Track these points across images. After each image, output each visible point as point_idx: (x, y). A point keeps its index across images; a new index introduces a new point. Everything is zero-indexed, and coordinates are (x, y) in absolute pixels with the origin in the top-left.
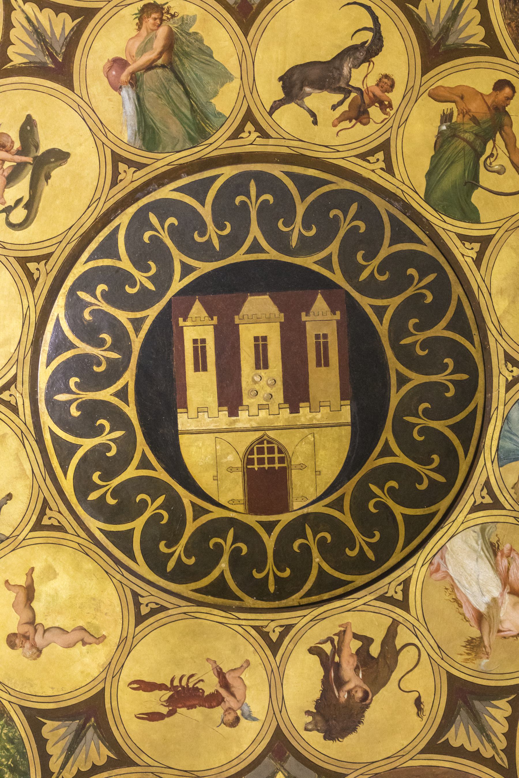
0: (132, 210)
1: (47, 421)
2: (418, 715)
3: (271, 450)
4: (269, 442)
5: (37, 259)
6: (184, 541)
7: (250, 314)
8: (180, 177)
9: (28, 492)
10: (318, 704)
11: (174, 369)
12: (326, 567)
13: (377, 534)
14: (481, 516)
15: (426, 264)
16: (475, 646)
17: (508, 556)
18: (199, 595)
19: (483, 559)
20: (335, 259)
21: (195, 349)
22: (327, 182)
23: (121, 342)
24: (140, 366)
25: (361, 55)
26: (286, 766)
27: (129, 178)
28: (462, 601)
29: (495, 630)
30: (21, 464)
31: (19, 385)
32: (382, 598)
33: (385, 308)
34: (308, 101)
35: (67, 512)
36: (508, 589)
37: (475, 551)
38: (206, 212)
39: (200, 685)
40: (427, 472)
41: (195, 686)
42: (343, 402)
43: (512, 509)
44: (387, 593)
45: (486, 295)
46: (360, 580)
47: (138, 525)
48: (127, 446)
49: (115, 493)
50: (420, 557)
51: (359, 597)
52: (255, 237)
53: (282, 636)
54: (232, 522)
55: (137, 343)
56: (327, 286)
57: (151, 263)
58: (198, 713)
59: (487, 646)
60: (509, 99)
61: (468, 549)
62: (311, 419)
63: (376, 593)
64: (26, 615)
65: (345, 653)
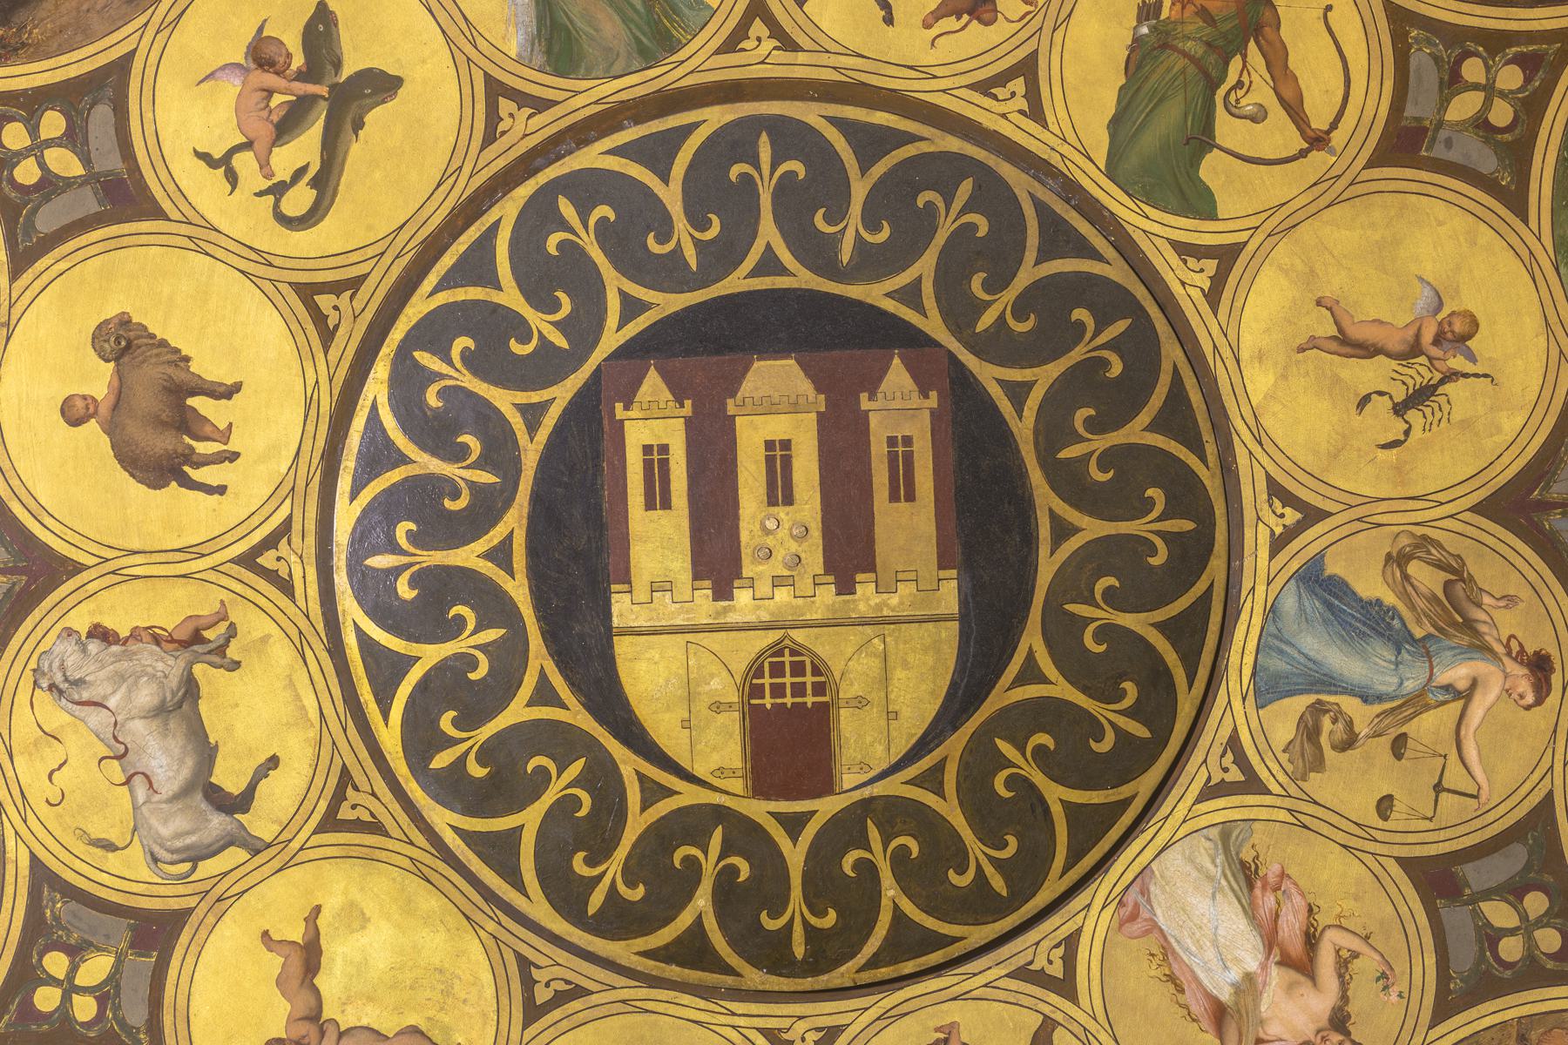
3: (798, 669)
4: (793, 653)
5: (336, 288)
6: (621, 853)
7: (757, 395)
8: (619, 128)
9: (310, 752)
11: (606, 506)
13: (1012, 842)
14: (1222, 809)
15: (1109, 301)
17: (1276, 889)
18: (652, 963)
19: (1225, 895)
20: (928, 288)
21: (648, 466)
22: (913, 138)
23: (500, 451)
24: (536, 498)
27: (519, 128)
28: (1184, 980)
30: (298, 697)
31: (296, 539)
32: (1023, 974)
33: (1028, 386)
35: (390, 795)
36: (1276, 955)
37: (1210, 878)
38: (671, 196)
40: (1111, 716)
42: (943, 574)
44: (1031, 963)
45: (1231, 363)
47: (530, 818)
48: (509, 658)
52: (768, 244)
54: (719, 814)
55: (531, 452)
56: (911, 340)
57: (560, 294)
61: (1195, 874)
62: (879, 607)
64: (305, 1001)
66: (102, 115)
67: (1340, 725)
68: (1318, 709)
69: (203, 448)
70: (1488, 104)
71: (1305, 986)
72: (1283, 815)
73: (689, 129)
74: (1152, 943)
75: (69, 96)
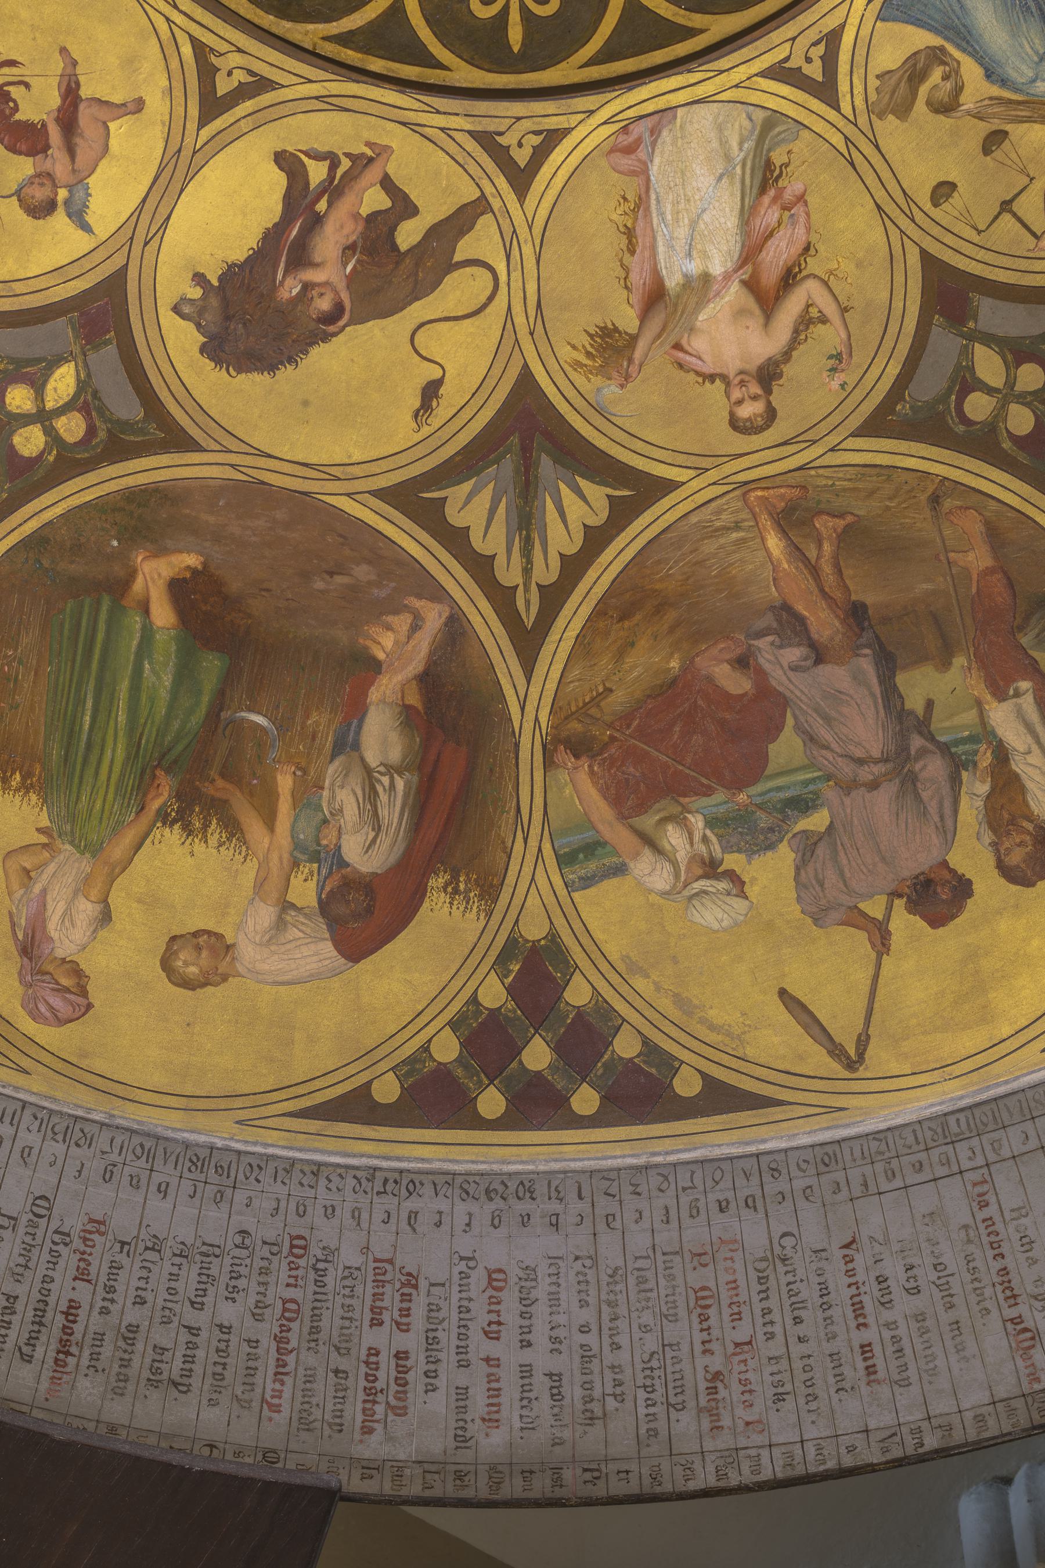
2: (416, 416)
10: (232, 273)
14: (781, 97)
16: (612, 348)
17: (785, 208)
19: (732, 183)
26: (92, 356)
28: (641, 242)
29: (672, 340)
32: (487, 140)
36: (745, 273)
37: (728, 158)
39: (15, 92)
41: (5, 88)
43: (851, 118)
44: (501, 134)
46: (466, 75)
50: (612, 103)
51: (441, 109)
53: (242, 93)
59: (637, 362)
61: (715, 144)
63: (480, 123)
67: (948, 85)
68: (937, 56)
71: (755, 322)
72: (837, 140)
74: (632, 187)
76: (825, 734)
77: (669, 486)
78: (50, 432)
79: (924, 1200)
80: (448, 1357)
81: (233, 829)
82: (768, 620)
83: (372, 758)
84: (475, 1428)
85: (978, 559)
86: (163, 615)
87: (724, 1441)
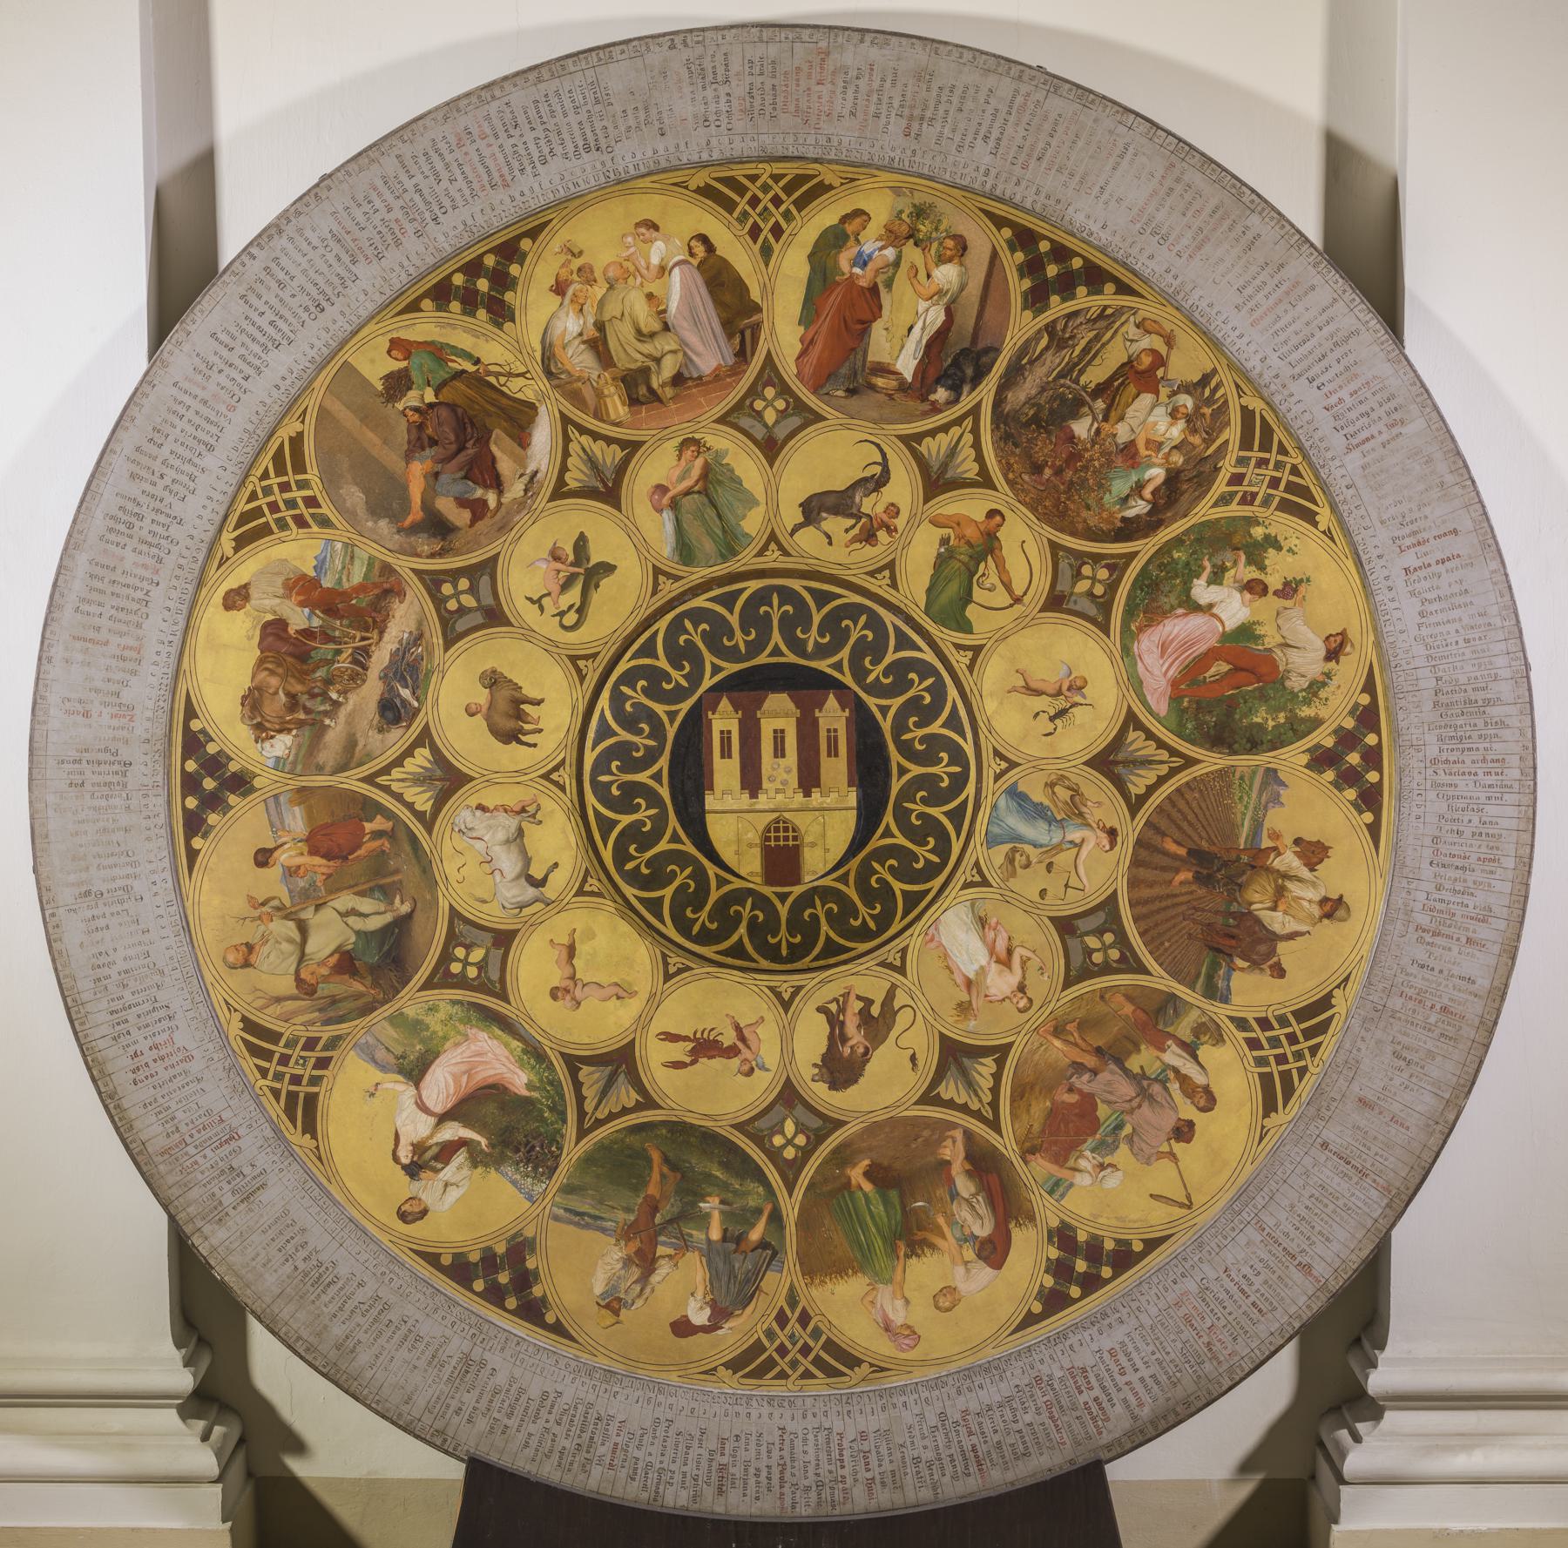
0: (670, 617)
1: (591, 799)
3: (786, 830)
5: (586, 657)
6: (708, 908)
10: (824, 1057)
12: (832, 934)
14: (972, 893)
16: (964, 1009)
21: (722, 739)
23: (658, 731)
24: (672, 753)
25: (871, 486)
27: (668, 588)
32: (883, 964)
34: (825, 525)
38: (734, 620)
47: (668, 892)
49: (649, 864)
54: (750, 892)
55: (671, 732)
56: (839, 686)
58: (717, 1063)
60: (1000, 526)
64: (568, 971)
65: (849, 1012)
66: (485, 579)
68: (1014, 850)
69: (527, 727)
70: (1093, 585)
73: (741, 591)
75: (472, 572)
76: (1113, 1098)
77: (1011, 1045)
78: (794, 1146)
79: (1242, 1239)
80: (1112, 1390)
81: (933, 1247)
82: (1071, 1070)
83: (966, 1195)
84: (1137, 1411)
85: (1128, 1009)
86: (868, 1187)
87: (1225, 1366)
